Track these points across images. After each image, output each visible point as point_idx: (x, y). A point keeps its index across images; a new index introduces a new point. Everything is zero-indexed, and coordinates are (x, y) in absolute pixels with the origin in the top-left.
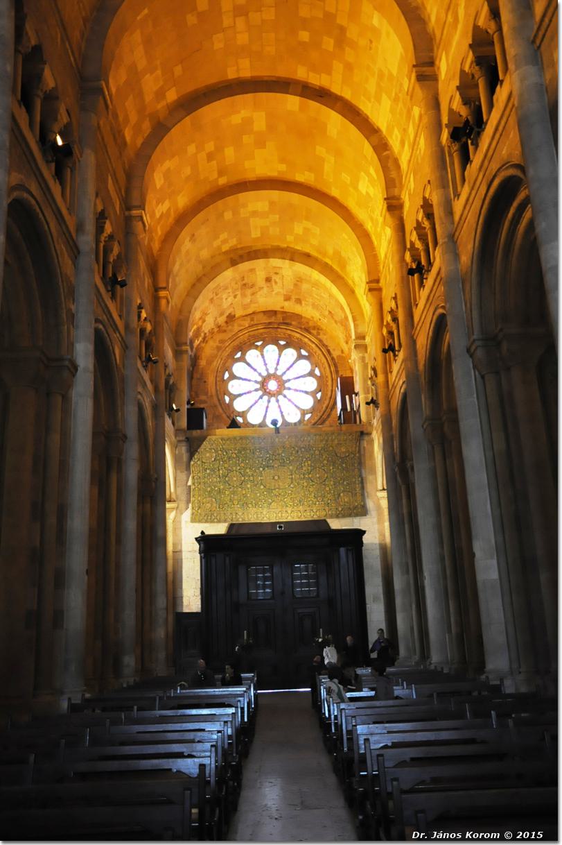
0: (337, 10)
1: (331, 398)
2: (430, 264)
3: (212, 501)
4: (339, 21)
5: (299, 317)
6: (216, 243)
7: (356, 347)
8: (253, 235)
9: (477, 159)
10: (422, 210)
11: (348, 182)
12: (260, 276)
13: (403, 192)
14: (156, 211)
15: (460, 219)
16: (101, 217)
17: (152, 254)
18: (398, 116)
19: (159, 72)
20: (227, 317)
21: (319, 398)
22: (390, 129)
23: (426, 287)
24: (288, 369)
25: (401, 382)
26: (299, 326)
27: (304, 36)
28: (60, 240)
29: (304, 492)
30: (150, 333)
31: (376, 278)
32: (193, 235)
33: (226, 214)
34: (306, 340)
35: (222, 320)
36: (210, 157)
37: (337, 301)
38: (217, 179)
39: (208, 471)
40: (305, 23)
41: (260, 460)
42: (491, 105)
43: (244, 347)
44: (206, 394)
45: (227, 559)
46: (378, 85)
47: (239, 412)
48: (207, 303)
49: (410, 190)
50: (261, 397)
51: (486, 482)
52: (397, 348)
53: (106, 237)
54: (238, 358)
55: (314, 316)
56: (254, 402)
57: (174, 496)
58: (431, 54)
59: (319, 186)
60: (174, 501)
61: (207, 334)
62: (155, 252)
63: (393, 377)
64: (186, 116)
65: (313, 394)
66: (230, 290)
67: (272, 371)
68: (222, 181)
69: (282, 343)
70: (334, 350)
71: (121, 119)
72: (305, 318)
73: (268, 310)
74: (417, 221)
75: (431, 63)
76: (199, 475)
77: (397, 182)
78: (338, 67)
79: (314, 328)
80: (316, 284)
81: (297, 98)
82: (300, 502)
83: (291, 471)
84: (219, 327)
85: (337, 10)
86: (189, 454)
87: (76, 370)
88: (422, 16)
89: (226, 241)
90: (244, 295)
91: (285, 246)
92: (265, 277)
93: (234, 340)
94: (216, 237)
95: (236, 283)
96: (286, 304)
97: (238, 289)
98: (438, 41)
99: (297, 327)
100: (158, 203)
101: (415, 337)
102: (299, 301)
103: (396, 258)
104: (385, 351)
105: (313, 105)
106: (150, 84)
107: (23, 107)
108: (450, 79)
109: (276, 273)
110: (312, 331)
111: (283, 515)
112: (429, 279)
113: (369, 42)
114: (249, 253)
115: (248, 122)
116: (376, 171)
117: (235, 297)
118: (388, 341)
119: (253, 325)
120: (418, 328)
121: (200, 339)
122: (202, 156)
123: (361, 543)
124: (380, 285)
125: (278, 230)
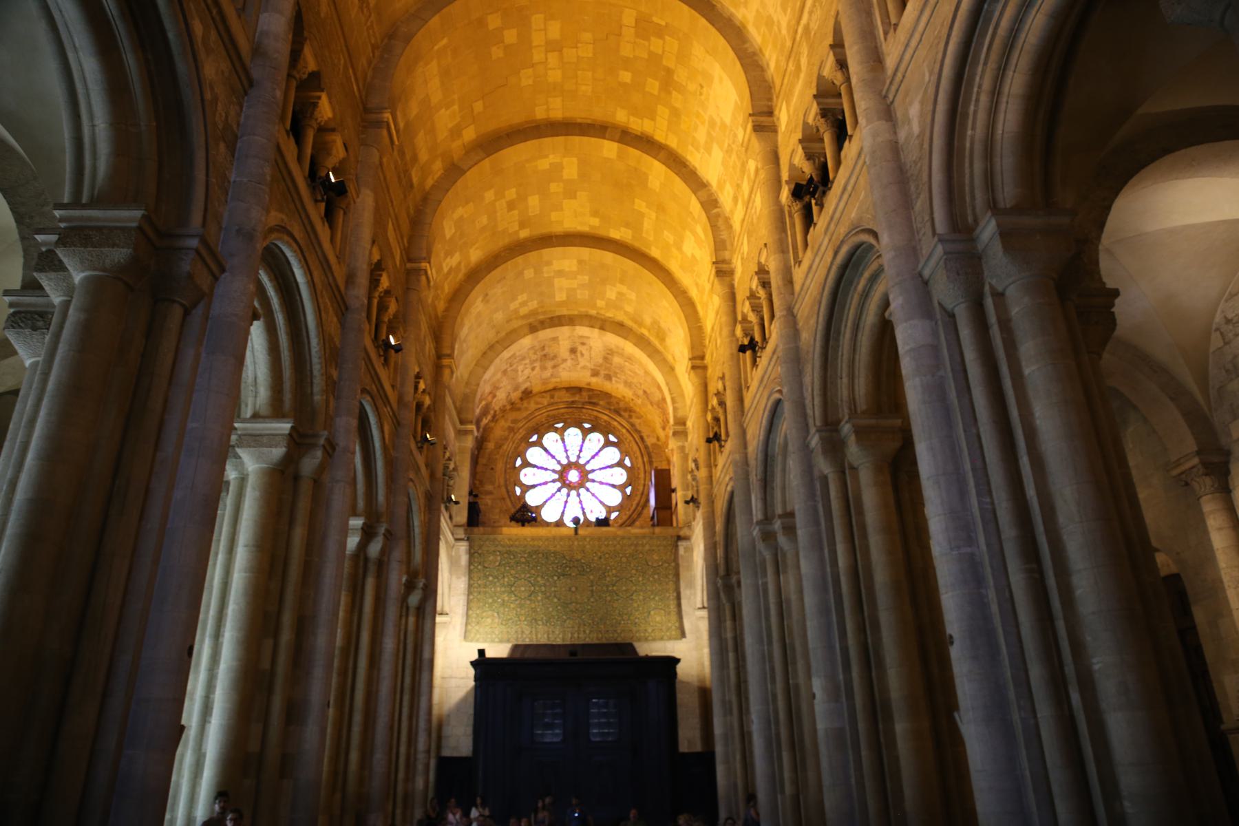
0: (663, 51)
1: (642, 494)
2: (764, 339)
3: (493, 615)
4: (665, 62)
5: (607, 396)
6: (513, 306)
7: (675, 434)
8: (558, 299)
9: (821, 221)
10: (756, 278)
11: (671, 242)
13: (735, 256)
14: (444, 265)
15: (802, 289)
17: (436, 316)
18: (731, 169)
19: (456, 107)
21: (628, 493)
23: (759, 368)
24: (593, 457)
25: (727, 478)
26: (608, 407)
27: (626, 77)
28: (324, 292)
30: (429, 408)
31: (698, 353)
32: (487, 295)
33: (525, 272)
34: (615, 423)
35: (516, 396)
36: (511, 206)
37: (654, 379)
38: (517, 232)
39: (491, 578)
40: (627, 63)
41: (555, 566)
42: (838, 163)
43: (541, 430)
46: (709, 133)
48: (499, 375)
49: (743, 254)
50: (559, 490)
52: (723, 437)
53: (381, 292)
55: (626, 395)
56: (550, 495)
57: (446, 609)
58: (770, 103)
59: (637, 244)
60: (447, 614)
61: (498, 413)
62: (440, 314)
63: (718, 472)
64: (485, 158)
65: (622, 488)
67: (573, 459)
68: (524, 234)
69: (587, 426)
70: (648, 436)
71: (408, 157)
72: (615, 397)
73: (573, 385)
74: (751, 290)
75: (770, 113)
76: (479, 582)
77: (728, 243)
78: (663, 112)
79: (626, 410)
80: (630, 359)
81: (615, 145)
82: (601, 619)
83: (592, 581)
84: (512, 404)
85: (663, 51)
87: (334, 449)
88: (760, 63)
89: (525, 303)
90: (543, 368)
92: (569, 347)
93: (529, 421)
94: (514, 299)
95: (535, 353)
96: (594, 380)
97: (537, 360)
98: (777, 88)
99: (604, 408)
103: (725, 332)
104: (709, 441)
106: (445, 120)
107: (291, 137)
108: (791, 132)
109: (583, 344)
110: (623, 413)
111: (580, 636)
112: (763, 358)
113: (699, 88)
114: (552, 319)
116: (705, 231)
117: (533, 369)
118: (713, 428)
120: (749, 415)
121: (489, 417)
122: (502, 205)
123: (675, 674)
124: (705, 362)
125: (587, 292)
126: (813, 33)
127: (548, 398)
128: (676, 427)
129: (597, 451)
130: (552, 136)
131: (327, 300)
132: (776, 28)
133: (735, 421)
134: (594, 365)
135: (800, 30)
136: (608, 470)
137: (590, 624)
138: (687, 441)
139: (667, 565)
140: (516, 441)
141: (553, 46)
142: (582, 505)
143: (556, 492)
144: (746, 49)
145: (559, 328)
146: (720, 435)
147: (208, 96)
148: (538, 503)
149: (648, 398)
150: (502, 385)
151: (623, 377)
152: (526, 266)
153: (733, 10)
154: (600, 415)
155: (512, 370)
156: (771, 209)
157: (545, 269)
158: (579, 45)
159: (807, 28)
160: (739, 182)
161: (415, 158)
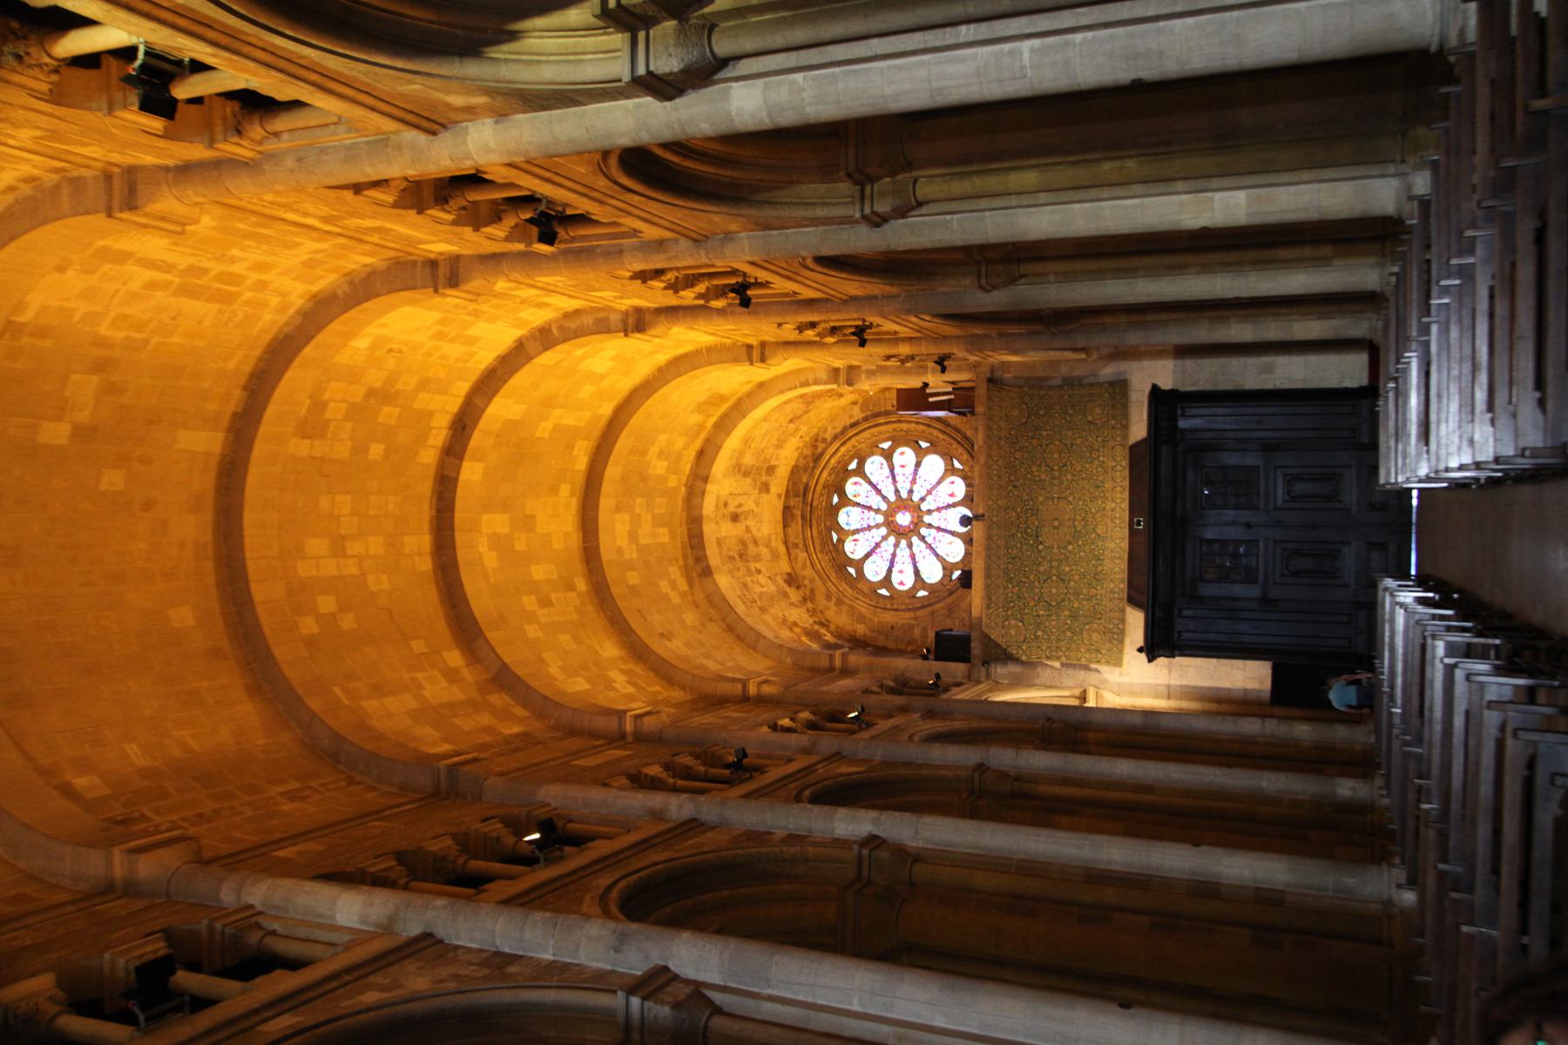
1: (929, 426)
2: (734, 272)
5: (795, 471)
6: (676, 599)
7: (850, 383)
9: (583, 205)
10: (650, 282)
12: (728, 530)
13: (618, 307)
14: (625, 691)
15: (672, 231)
16: (640, 782)
17: (693, 702)
19: (420, 676)
20: (790, 585)
22: (519, 324)
23: (770, 280)
24: (879, 492)
25: (914, 319)
26: (810, 470)
27: (376, 450)
28: (677, 848)
29: (1083, 479)
30: (813, 713)
31: (744, 351)
32: (662, 634)
33: (631, 582)
34: (833, 461)
35: (794, 595)
38: (580, 594)
39: (1039, 633)
40: (360, 449)
42: (512, 185)
43: (840, 561)
44: (911, 627)
45: (1187, 613)
46: (453, 340)
47: (944, 575)
48: (767, 618)
49: (615, 297)
50: (923, 539)
51: (1087, 205)
52: (860, 323)
53: (669, 776)
54: (857, 572)
55: (794, 446)
58: (419, 264)
59: (596, 433)
62: (688, 697)
63: (903, 331)
64: (485, 637)
66: (748, 579)
67: (880, 519)
68: (581, 585)
69: (836, 499)
71: (489, 739)
72: (797, 460)
73: (781, 519)
74: (665, 288)
75: (433, 264)
76: (1044, 648)
77: (600, 315)
78: (423, 401)
79: (815, 447)
80: (746, 442)
82: (1097, 487)
83: (1047, 498)
84: (805, 599)
85: (344, 401)
86: (1009, 662)
87: (876, 837)
88: (363, 276)
90: (757, 558)
91: (683, 489)
92: (730, 523)
94: (666, 598)
96: (774, 490)
98: (400, 254)
99: (812, 475)
100: (614, 689)
101: (845, 298)
102: (771, 470)
104: (863, 343)
105: (476, 440)
106: (438, 690)
107: (486, 887)
109: (726, 504)
110: (819, 450)
113: (392, 354)
115: (497, 541)
116: (583, 346)
117: (759, 572)
118: (845, 335)
119: (806, 546)
120: (832, 293)
121: (823, 631)
124: (755, 343)
125: (658, 500)
126: (335, 213)
127: (795, 551)
128: (841, 381)
129: (869, 488)
130: (454, 549)
131: (686, 844)
132: (319, 256)
133: (839, 311)
134: (755, 489)
135: (327, 228)
136: (896, 471)
137: (1103, 502)
138: (860, 367)
139: (1026, 398)
140: (857, 596)
141: (338, 548)
142: (943, 508)
143: (925, 542)
144: (345, 293)
145: (706, 538)
146: (857, 327)
147: (452, 985)
148: (939, 566)
149: (799, 417)
150: (780, 614)
151: (771, 450)
152: (623, 579)
153: (292, 311)
154: (822, 480)
155: (760, 599)
156: (562, 265)
157: (627, 556)
158: (336, 513)
159: (326, 220)
160: (518, 301)
161: (489, 730)
